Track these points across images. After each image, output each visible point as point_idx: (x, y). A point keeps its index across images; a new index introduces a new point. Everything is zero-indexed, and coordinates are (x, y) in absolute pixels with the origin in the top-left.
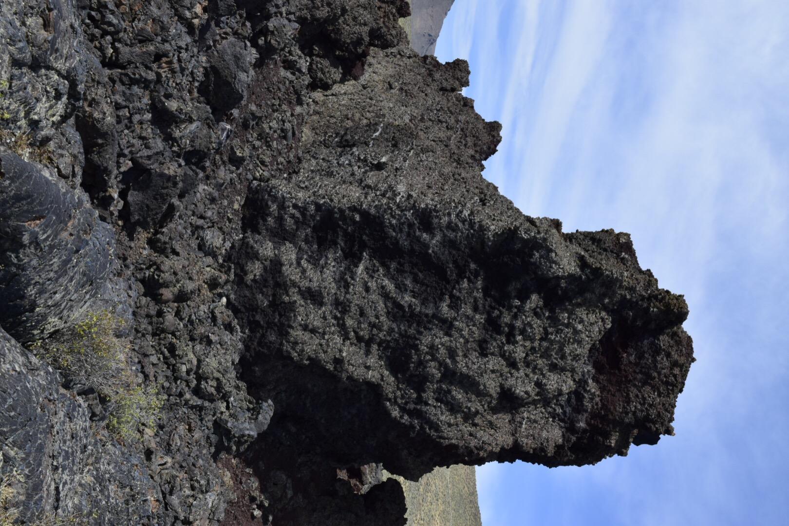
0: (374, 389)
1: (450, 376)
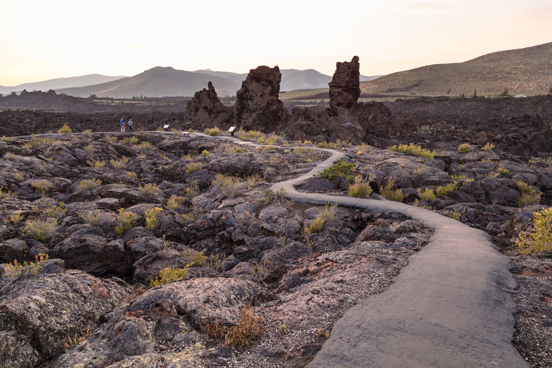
0: (257, 115)
1: (256, 105)
